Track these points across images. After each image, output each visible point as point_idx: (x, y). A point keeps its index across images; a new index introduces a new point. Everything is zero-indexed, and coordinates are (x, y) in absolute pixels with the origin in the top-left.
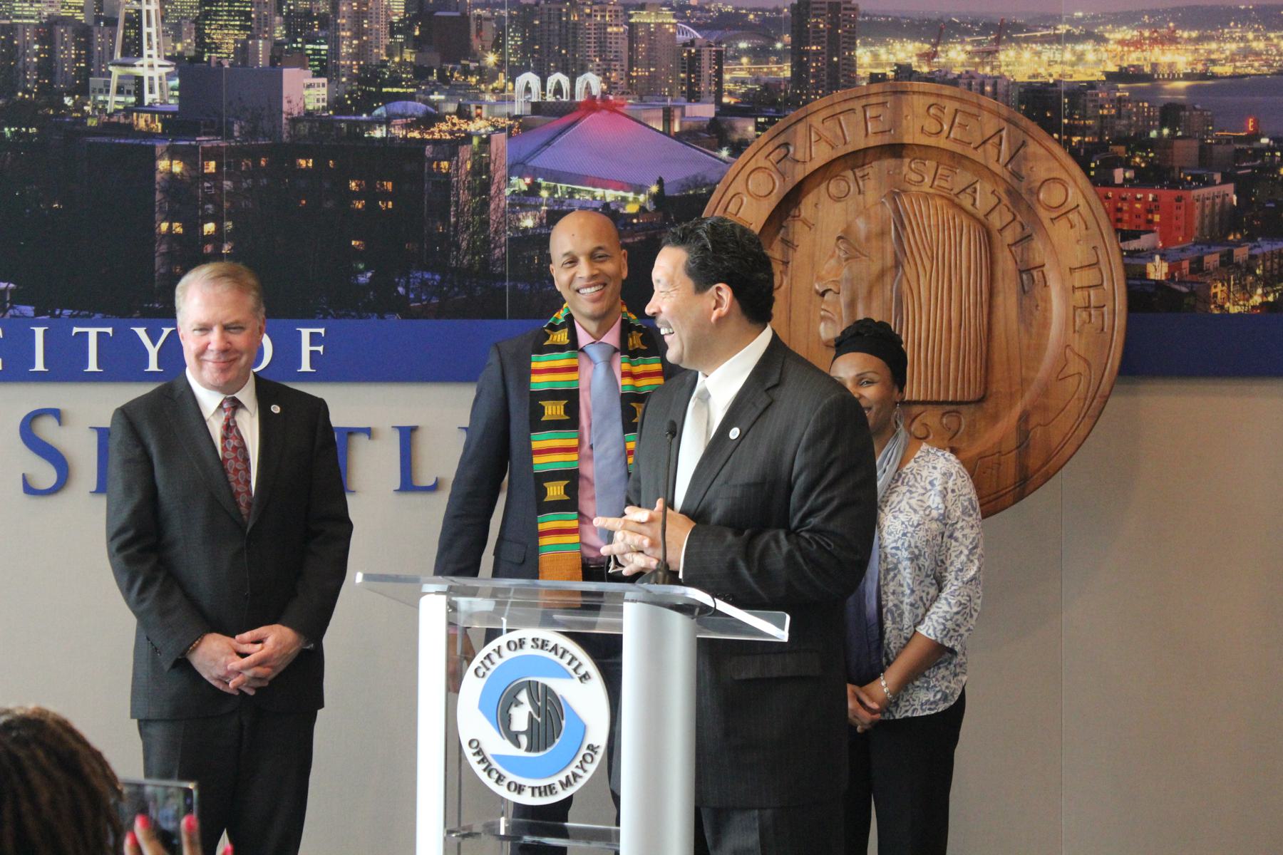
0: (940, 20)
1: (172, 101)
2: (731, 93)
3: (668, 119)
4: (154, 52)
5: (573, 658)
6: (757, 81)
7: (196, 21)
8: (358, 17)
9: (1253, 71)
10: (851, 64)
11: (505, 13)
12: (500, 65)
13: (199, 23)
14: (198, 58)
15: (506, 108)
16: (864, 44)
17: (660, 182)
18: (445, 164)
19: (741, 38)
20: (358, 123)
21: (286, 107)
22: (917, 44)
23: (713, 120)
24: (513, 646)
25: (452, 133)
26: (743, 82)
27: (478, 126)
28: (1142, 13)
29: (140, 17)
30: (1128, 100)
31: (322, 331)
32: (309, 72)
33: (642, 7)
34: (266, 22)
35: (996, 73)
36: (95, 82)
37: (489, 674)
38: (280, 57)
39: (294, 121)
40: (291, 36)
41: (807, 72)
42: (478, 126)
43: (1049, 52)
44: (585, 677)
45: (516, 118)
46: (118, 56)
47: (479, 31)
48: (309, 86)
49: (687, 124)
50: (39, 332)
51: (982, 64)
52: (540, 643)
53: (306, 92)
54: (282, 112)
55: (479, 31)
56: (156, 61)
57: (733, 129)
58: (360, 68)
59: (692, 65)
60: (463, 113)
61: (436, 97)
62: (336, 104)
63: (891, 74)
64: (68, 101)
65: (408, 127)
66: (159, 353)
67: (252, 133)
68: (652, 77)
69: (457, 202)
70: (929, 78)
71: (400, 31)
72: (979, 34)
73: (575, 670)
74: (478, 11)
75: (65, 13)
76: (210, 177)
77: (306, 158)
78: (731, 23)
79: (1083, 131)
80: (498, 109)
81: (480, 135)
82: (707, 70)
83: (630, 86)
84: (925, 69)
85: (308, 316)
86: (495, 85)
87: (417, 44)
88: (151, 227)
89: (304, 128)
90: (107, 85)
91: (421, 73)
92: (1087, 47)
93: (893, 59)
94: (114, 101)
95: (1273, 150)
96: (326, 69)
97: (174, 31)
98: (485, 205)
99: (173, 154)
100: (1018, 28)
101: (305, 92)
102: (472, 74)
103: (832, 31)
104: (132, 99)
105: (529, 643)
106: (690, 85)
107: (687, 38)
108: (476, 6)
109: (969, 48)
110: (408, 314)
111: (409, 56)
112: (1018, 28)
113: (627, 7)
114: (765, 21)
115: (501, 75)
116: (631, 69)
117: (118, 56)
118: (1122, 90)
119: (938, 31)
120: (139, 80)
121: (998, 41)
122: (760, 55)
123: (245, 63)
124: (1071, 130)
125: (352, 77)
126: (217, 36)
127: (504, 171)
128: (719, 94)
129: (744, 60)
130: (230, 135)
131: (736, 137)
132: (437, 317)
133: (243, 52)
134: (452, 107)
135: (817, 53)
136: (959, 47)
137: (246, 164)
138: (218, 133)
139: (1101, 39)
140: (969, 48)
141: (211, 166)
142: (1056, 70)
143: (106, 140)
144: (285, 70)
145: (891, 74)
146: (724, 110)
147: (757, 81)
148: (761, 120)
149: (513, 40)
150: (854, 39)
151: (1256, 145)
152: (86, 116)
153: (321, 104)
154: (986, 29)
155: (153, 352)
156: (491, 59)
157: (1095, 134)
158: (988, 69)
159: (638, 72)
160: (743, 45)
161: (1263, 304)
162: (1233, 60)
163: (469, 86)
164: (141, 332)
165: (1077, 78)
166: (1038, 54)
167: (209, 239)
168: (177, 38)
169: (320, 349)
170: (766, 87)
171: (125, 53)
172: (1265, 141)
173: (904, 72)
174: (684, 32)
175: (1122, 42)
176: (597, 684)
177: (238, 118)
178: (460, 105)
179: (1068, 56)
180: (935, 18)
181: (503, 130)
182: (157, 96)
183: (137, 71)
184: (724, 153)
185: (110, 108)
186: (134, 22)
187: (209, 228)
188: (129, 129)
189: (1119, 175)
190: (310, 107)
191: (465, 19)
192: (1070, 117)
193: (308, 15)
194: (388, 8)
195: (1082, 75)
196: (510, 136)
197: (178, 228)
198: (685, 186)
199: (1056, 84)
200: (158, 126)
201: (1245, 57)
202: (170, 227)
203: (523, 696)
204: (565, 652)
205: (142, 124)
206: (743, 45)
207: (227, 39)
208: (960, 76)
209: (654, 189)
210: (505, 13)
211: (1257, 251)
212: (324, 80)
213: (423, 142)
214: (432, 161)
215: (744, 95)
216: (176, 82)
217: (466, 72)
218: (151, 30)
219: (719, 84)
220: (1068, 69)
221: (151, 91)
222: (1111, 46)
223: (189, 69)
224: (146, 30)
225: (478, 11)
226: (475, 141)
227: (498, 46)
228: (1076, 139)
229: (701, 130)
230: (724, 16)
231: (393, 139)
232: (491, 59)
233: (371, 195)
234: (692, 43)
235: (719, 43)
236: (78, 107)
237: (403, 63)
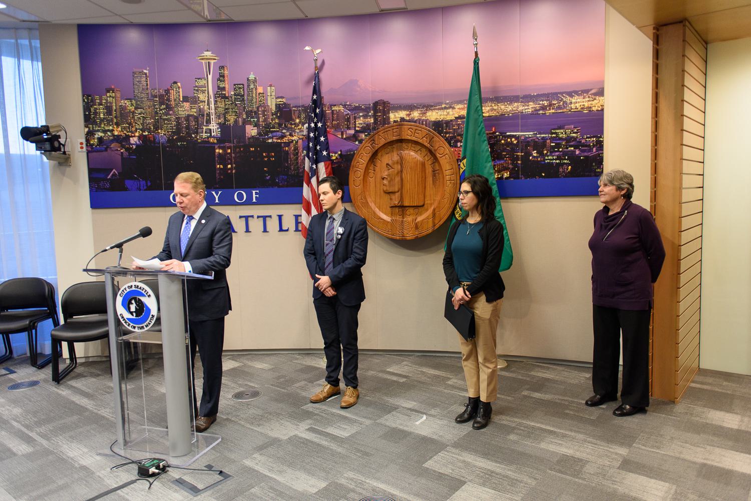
0: (411, 105)
2: (358, 127)
3: (342, 134)
4: (214, 122)
6: (365, 123)
7: (223, 114)
8: (264, 111)
9: (494, 115)
10: (389, 118)
11: (300, 109)
12: (300, 122)
13: (224, 115)
14: (225, 123)
15: (302, 133)
16: (392, 112)
17: (341, 151)
18: (287, 148)
19: (360, 113)
20: (265, 139)
21: (247, 135)
22: (406, 112)
23: (354, 134)
25: (288, 140)
26: (361, 124)
27: (295, 138)
28: (464, 100)
29: (210, 114)
30: (461, 124)
31: (258, 191)
32: (252, 126)
33: (335, 105)
34: (241, 114)
35: (426, 119)
36: (200, 130)
38: (245, 122)
39: (249, 139)
40: (247, 117)
41: (377, 120)
42: (295, 138)
43: (440, 112)
45: (304, 136)
46: (205, 124)
47: (294, 113)
48: (252, 130)
49: (347, 135)
51: (423, 116)
53: (252, 131)
54: (246, 136)
55: (294, 113)
56: (214, 125)
57: (359, 136)
58: (265, 124)
59: (348, 120)
60: (291, 135)
61: (284, 131)
62: (259, 134)
63: (399, 120)
64: (193, 136)
65: (277, 139)
67: (239, 142)
68: (338, 123)
69: (290, 158)
70: (409, 121)
71: (274, 114)
72: (422, 108)
74: (294, 109)
75: (192, 113)
76: (229, 153)
77: (252, 148)
78: (357, 109)
79: (449, 133)
80: (300, 134)
81: (295, 140)
82: (352, 121)
83: (333, 126)
84: (408, 118)
85: (255, 188)
86: (299, 127)
87: (279, 118)
88: (215, 167)
89: (251, 140)
90: (203, 131)
91: (280, 125)
92: (450, 110)
93: (399, 116)
94: (204, 135)
95: (500, 136)
96: (256, 125)
97: (219, 117)
98: (297, 158)
99: (220, 148)
100: (432, 106)
101: (252, 131)
102: (293, 125)
103: (384, 110)
104: (209, 135)
106: (348, 126)
107: (346, 113)
108: (293, 107)
109: (419, 112)
110: (279, 187)
111: (277, 121)
112: (432, 106)
113: (331, 106)
114: (366, 107)
115: (300, 125)
116: (333, 122)
117: (205, 124)
118: (460, 121)
119: (410, 108)
121: (427, 110)
122: (365, 117)
123: (236, 124)
124: (446, 133)
125: (263, 127)
126: (229, 118)
127: (301, 149)
128: (355, 127)
129: (361, 118)
130: (233, 143)
131: (360, 138)
132: (287, 187)
133: (236, 121)
134: (288, 134)
135: (380, 115)
136: (416, 112)
137: (238, 150)
138: (230, 142)
139: (454, 108)
140: (419, 112)
141: (229, 151)
142: (442, 117)
143: (203, 145)
144: (246, 126)
145: (399, 120)
146: (357, 132)
147: (365, 123)
148: (366, 134)
149: (303, 116)
150: (389, 111)
151: (495, 135)
152: (198, 139)
153: (255, 134)
154: (423, 108)
155: (217, 198)
156: (298, 121)
157: (452, 134)
158: (424, 118)
159: (334, 122)
160: (361, 114)
161: (497, 178)
162: (489, 112)
163: (292, 128)
164: (214, 193)
165: (448, 119)
166: (437, 113)
167: (229, 169)
168: (219, 119)
169: (258, 196)
170: (367, 125)
171: (207, 123)
172: (497, 133)
173: (402, 119)
174: (345, 111)
175: (459, 109)
177: (235, 138)
178: (290, 133)
179: (445, 113)
180: (410, 104)
181: (301, 139)
182: (215, 133)
183: (210, 127)
184: (357, 143)
185: (203, 137)
186: (209, 115)
187: (229, 166)
188: (208, 142)
189: (459, 144)
190: (253, 135)
191: (291, 110)
192: (446, 129)
193: (251, 111)
194: (271, 109)
195: (449, 118)
196: (303, 140)
197: (222, 167)
198: (347, 151)
199: (442, 121)
200: (216, 141)
201: (492, 111)
202: (220, 167)
205: (212, 141)
206: (361, 114)
207: (231, 119)
208: (417, 120)
209: (339, 153)
210: (300, 109)
211: (495, 164)
212: (256, 128)
213: (281, 142)
214: (283, 148)
215: (361, 127)
216: (220, 130)
217: (291, 124)
218: (213, 117)
219: (355, 125)
220: (445, 117)
221: (214, 132)
222: (456, 110)
223: (223, 126)
224: (211, 117)
225: (294, 109)
226: (294, 142)
227: (299, 117)
228: (447, 135)
229: (351, 137)
230: (356, 107)
231: (274, 142)
232: (298, 121)
233: (268, 156)
234: (348, 114)
235: (355, 114)
236: (196, 137)
237: (275, 123)
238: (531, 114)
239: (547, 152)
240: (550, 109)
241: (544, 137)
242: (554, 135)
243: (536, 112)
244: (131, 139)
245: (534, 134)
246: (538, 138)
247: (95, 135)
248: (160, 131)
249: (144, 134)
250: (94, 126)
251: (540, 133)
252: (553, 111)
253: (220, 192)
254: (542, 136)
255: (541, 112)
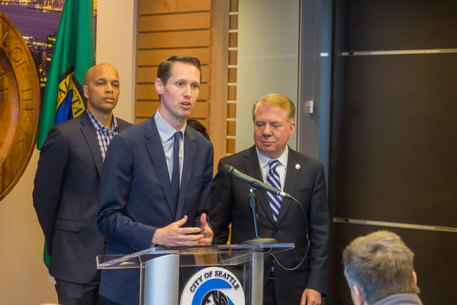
5: (232, 278)
24: (207, 276)
37: (196, 290)
44: (237, 287)
52: (218, 273)
73: (233, 284)
105: (214, 273)
176: (241, 290)
203: (211, 298)
204: (229, 276)
238: (28, 8)
239: (43, 72)
240: (46, 5)
241: (39, 47)
242: (50, 46)
243: (32, 6)
245: (30, 39)
246: (33, 47)
251: (37, 40)
252: (49, 7)
254: (38, 44)
255: (38, 6)
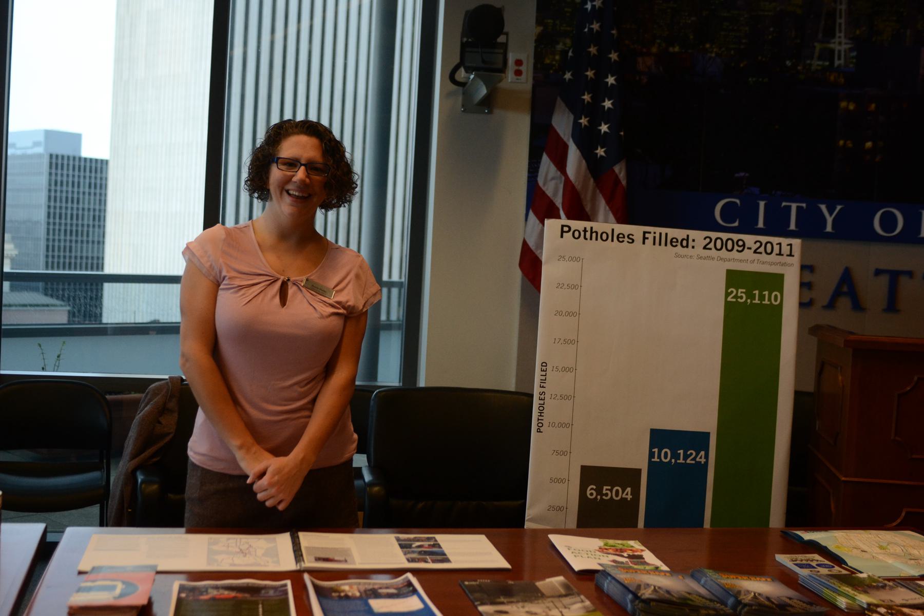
1: (851, 66)
4: (842, 35)
46: (820, 36)
50: (762, 204)
56: (843, 40)
64: (788, 63)
66: (834, 221)
94: (816, 64)
117: (820, 36)
120: (832, 51)
155: (830, 220)
164: (823, 207)
182: (842, 61)
183: (832, 46)
197: (850, 144)
200: (842, 80)
202: (845, 143)
218: (841, 21)
221: (839, 59)
224: (838, 21)
244: (640, 60)
247: (558, 43)
248: (708, 46)
249: (671, 49)
250: (558, 22)
253: (839, 207)
